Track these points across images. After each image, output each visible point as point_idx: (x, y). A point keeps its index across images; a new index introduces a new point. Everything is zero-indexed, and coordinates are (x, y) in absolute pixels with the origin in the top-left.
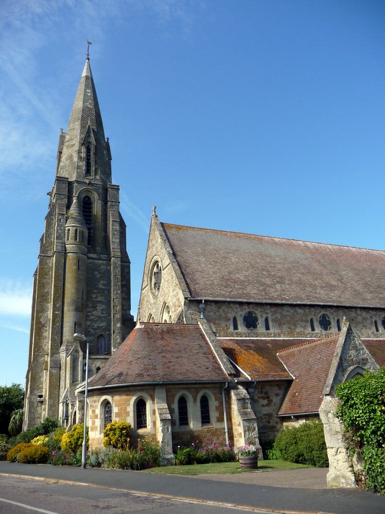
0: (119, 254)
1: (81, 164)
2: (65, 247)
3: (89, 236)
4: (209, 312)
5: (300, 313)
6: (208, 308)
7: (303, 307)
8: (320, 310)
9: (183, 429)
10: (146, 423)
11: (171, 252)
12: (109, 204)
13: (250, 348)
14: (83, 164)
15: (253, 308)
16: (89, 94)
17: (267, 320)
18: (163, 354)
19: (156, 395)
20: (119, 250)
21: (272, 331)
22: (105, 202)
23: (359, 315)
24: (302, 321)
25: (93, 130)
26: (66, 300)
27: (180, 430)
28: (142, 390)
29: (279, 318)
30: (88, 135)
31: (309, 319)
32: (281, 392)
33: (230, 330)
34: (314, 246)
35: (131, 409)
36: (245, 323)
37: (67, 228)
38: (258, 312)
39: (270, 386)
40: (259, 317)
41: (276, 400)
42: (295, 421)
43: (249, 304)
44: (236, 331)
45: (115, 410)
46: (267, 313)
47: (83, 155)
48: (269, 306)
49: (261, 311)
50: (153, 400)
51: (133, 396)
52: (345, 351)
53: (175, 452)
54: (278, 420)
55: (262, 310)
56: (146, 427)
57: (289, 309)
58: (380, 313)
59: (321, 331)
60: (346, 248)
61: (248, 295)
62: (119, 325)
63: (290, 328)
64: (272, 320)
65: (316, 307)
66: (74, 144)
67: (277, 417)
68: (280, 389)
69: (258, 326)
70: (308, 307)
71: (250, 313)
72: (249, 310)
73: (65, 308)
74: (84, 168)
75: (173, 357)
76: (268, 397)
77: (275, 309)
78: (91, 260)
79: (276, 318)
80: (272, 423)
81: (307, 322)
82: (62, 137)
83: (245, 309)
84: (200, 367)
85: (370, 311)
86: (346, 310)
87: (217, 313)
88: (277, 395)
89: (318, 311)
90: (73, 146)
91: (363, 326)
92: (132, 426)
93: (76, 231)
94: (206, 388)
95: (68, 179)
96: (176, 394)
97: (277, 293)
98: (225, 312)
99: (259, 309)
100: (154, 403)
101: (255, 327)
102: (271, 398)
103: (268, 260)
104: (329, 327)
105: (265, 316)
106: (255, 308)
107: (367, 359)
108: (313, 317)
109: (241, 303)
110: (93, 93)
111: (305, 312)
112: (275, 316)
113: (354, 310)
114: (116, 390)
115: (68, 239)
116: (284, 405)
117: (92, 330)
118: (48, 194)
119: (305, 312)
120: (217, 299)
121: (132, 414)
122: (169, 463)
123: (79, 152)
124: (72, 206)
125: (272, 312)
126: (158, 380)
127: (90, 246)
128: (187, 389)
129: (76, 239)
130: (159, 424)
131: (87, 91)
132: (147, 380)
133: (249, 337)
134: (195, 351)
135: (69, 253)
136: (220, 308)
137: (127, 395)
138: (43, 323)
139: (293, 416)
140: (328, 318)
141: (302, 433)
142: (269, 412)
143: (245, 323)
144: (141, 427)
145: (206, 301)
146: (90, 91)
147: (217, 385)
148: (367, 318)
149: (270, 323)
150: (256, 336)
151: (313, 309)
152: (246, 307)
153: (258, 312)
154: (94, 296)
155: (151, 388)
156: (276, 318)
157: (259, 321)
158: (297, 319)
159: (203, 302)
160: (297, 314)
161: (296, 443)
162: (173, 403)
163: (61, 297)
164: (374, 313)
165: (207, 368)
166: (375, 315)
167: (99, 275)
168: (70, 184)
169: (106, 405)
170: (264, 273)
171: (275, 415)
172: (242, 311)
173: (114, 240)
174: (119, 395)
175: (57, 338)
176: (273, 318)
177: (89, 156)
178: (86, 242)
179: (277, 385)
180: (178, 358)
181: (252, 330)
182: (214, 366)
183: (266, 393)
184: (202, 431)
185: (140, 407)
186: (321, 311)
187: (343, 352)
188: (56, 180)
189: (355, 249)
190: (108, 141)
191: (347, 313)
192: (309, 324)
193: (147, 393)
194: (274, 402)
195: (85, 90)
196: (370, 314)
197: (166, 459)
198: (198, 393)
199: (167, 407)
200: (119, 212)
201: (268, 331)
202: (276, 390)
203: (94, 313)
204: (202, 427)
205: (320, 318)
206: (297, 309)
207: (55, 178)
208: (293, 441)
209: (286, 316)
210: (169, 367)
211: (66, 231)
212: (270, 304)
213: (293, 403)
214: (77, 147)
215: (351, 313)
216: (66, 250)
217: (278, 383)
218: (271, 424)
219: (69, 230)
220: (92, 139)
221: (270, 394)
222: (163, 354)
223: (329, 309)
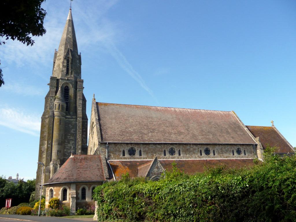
0: (81, 116)
1: (64, 69)
2: (54, 114)
3: (67, 107)
6: (110, 146)
7: (161, 145)
8: (170, 145)
9: (83, 201)
10: (66, 199)
11: (98, 118)
12: (78, 89)
14: (65, 69)
15: (133, 146)
16: (70, 30)
17: (140, 152)
18: (79, 170)
19: (71, 187)
20: (81, 114)
21: (142, 156)
22: (76, 88)
23: (191, 147)
24: (159, 151)
25: (71, 50)
27: (81, 202)
28: (66, 185)
30: (68, 53)
31: (163, 150)
33: (120, 156)
34: (180, 111)
35: (60, 193)
37: (55, 104)
38: (136, 148)
40: (136, 150)
43: (131, 144)
44: (124, 157)
45: (54, 193)
46: (141, 148)
47: (65, 64)
48: (142, 145)
49: (138, 147)
50: (70, 189)
51: (61, 187)
52: (152, 169)
53: (76, 210)
56: (66, 200)
57: (153, 145)
58: (204, 146)
60: (199, 110)
61: (132, 140)
63: (152, 155)
64: (143, 151)
65: (168, 144)
66: (61, 58)
69: (136, 154)
72: (131, 147)
74: (65, 71)
75: (83, 170)
77: (145, 146)
78: (67, 119)
79: (145, 150)
81: (162, 151)
82: (56, 54)
83: (129, 146)
84: (94, 175)
85: (198, 145)
86: (184, 145)
87: (115, 149)
89: (169, 146)
90: (60, 59)
91: (193, 153)
92: (60, 200)
93: (59, 105)
94: (95, 184)
95: (56, 78)
96: (80, 187)
97: (148, 138)
98: (119, 148)
99: (137, 146)
100: (70, 190)
101: (134, 154)
103: (150, 119)
104: (174, 154)
105: (139, 149)
106: (134, 145)
108: (166, 149)
109: (127, 144)
110: (72, 29)
111: (161, 147)
112: (145, 149)
113: (189, 145)
114: (56, 185)
115: (55, 109)
117: (67, 154)
118: (48, 85)
119: (161, 147)
120: (114, 142)
121: (60, 195)
122: (74, 214)
123: (63, 63)
125: (143, 147)
126: (72, 181)
127: (67, 112)
128: (86, 185)
129: (59, 109)
130: (71, 199)
131: (69, 28)
132: (68, 181)
133: (130, 159)
134: (94, 168)
136: (116, 146)
137: (59, 187)
138: (43, 150)
140: (174, 149)
144: (65, 200)
145: (108, 143)
146: (70, 28)
147: (100, 183)
148: (196, 149)
152: (130, 145)
153: (136, 148)
157: (136, 152)
158: (157, 150)
159: (107, 143)
160: (157, 148)
164: (201, 146)
165: (97, 175)
166: (200, 147)
168: (58, 80)
169: (51, 191)
170: (145, 127)
172: (127, 147)
173: (79, 109)
174: (56, 187)
176: (144, 150)
178: (65, 110)
180: (85, 171)
181: (132, 156)
182: (101, 174)
184: (91, 202)
185: (65, 192)
186: (170, 146)
189: (204, 111)
191: (185, 147)
192: (163, 153)
193: (67, 186)
196: (198, 147)
197: (72, 213)
199: (75, 192)
200: (83, 94)
201: (140, 157)
204: (92, 200)
205: (170, 149)
207: (50, 78)
209: (151, 149)
210: (79, 175)
211: (55, 105)
212: (143, 144)
214: (62, 60)
216: (54, 115)
219: (56, 105)
222: (79, 170)
223: (175, 145)
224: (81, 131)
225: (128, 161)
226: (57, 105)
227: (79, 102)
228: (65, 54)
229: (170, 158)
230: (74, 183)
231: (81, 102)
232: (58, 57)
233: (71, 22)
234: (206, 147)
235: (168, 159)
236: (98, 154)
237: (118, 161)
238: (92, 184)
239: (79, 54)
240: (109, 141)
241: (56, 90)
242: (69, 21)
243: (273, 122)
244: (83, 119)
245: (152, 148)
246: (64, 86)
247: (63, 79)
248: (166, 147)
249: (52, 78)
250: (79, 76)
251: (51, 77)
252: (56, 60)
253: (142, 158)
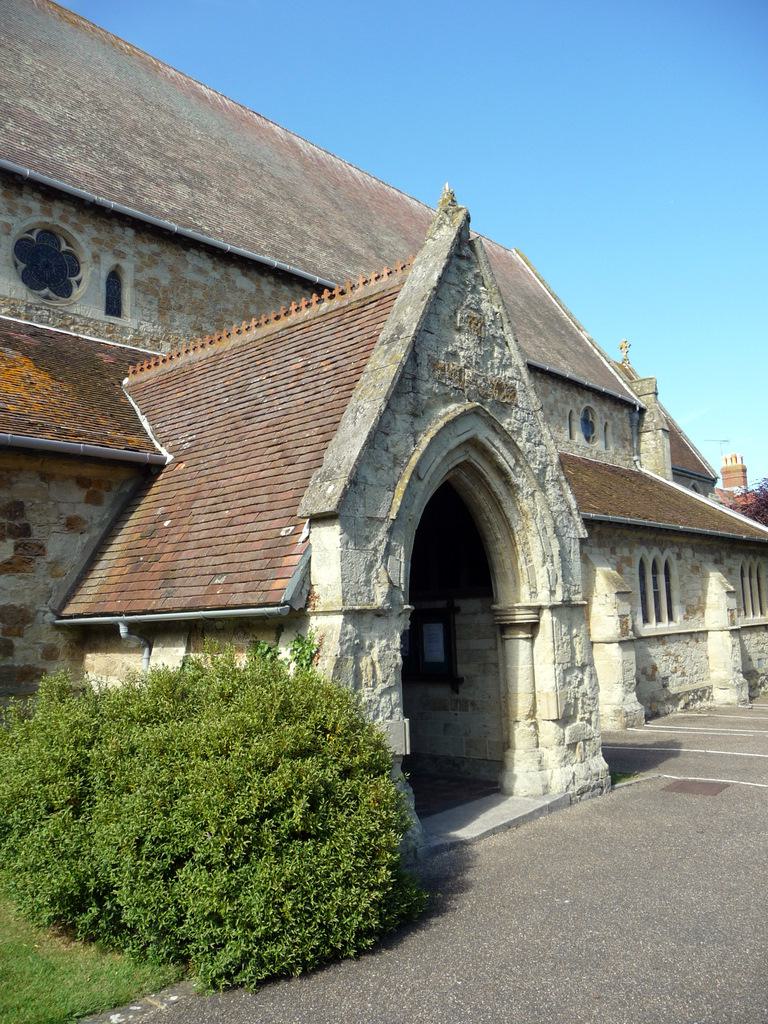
5: (243, 291)
13: (11, 343)
15: (63, 218)
17: (114, 280)
21: (129, 321)
29: (165, 282)
32: (97, 515)
34: (315, 154)
36: (23, 266)
38: (84, 240)
39: (45, 477)
40: (85, 254)
41: (63, 547)
42: (138, 649)
43: (50, 194)
46: (120, 254)
48: (130, 232)
49: (96, 240)
52: (434, 326)
54: (61, 641)
55: (104, 236)
57: (207, 264)
60: (396, 192)
61: (58, 169)
63: (200, 329)
67: (58, 627)
68: (93, 499)
69: (77, 292)
70: (272, 279)
71: (49, 234)
76: (26, 531)
77: (155, 247)
79: (154, 280)
80: (25, 653)
83: (29, 210)
88: (73, 524)
97: (173, 205)
101: (65, 291)
102: (37, 534)
103: (165, 119)
105: (108, 262)
106: (73, 219)
107: (513, 392)
111: (259, 290)
112: (149, 273)
116: (101, 571)
125: (140, 254)
139: (131, 626)
141: (137, 735)
142: (17, 603)
143: (23, 266)
149: (128, 295)
150: (58, 321)
152: (35, 205)
153: (84, 240)
156: (154, 280)
157: (85, 273)
158: (230, 307)
160: (234, 289)
161: (79, 803)
170: (142, 141)
171: (50, 617)
176: (143, 277)
179: (82, 482)
181: (47, 297)
183: (17, 509)
187: (424, 329)
189: (416, 203)
194: (51, 556)
201: (113, 319)
202: (72, 501)
206: (235, 273)
208: (61, 792)
209: (194, 285)
213: (137, 561)
217: (90, 471)
218: (18, 660)
221: (32, 517)
243: (626, 347)
245: (199, 279)
253: (124, 329)
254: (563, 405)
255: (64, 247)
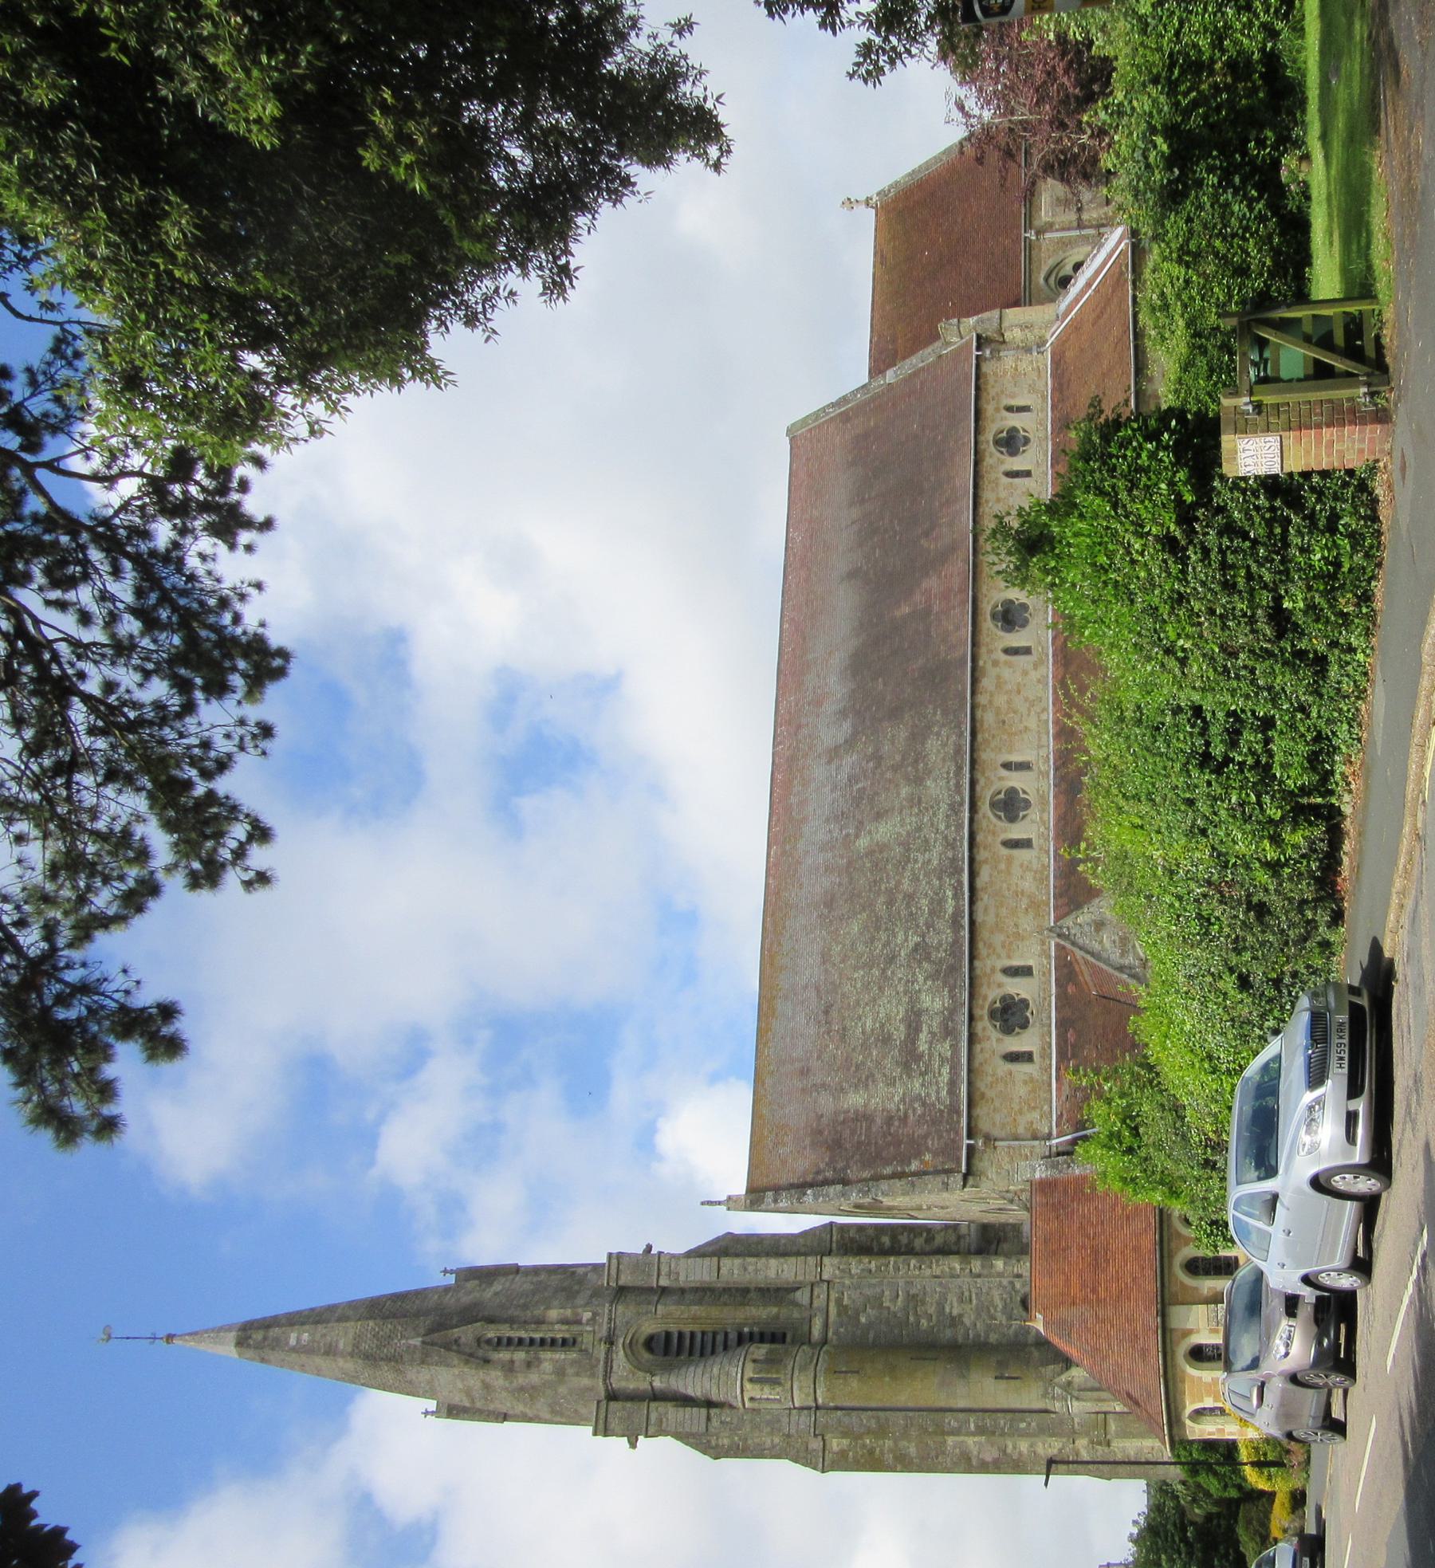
1: (547, 1366)
2: (802, 1408)
3: (762, 1338)
4: (994, 1124)
6: (984, 1125)
7: (976, 865)
11: (839, 1187)
12: (664, 1282)
14: (550, 1359)
15: (982, 1008)
23: (990, 702)
25: (430, 1331)
26: (942, 1404)
28: (1173, 1352)
29: (1002, 938)
31: (1005, 851)
33: (1036, 1075)
38: (992, 993)
43: (971, 1018)
44: (1036, 1057)
45: (1209, 1403)
46: (993, 970)
47: (520, 1356)
51: (1184, 1372)
55: (984, 981)
57: (980, 906)
59: (1033, 821)
62: (999, 1264)
64: (1009, 957)
65: (975, 826)
66: (483, 1381)
69: (1024, 995)
73: (962, 1404)
74: (560, 1356)
77: (980, 945)
78: (830, 1334)
83: (984, 1029)
85: (981, 663)
86: (980, 737)
87: (997, 1104)
89: (984, 824)
90: (487, 1386)
91: (1019, 692)
93: (751, 1380)
96: (1182, 1283)
100: (1198, 1331)
105: (1001, 978)
106: (981, 1002)
112: (999, 949)
113: (979, 713)
115: (779, 1401)
123: (509, 1368)
124: (682, 1390)
127: (789, 1339)
128: (1171, 1257)
129: (775, 1382)
131: (293, 1341)
132: (1154, 1344)
135: (816, 1399)
136: (983, 1095)
137: (1183, 1382)
145: (969, 1137)
148: (998, 677)
149: (1016, 962)
151: (979, 838)
153: (992, 993)
154: (924, 1322)
155: (1167, 1335)
162: (1196, 1289)
163: (933, 1415)
164: (983, 650)
166: (990, 652)
167: (869, 1310)
172: (989, 1038)
175: (1034, 1421)
176: (1003, 954)
177: (521, 1341)
188: (605, 1435)
190: (451, 1272)
192: (1016, 852)
195: (294, 1350)
196: (989, 666)
198: (1179, 1235)
199: (1202, 1308)
200: (690, 1254)
203: (967, 1321)
205: (999, 818)
207: (600, 1438)
209: (997, 916)
211: (756, 1405)
214: (495, 1377)
215: (986, 726)
216: (809, 1408)
219: (752, 1399)
220: (466, 1334)
224: (892, 1259)
225: (1058, 1036)
226: (753, 1394)
227: (733, 1270)
228: (455, 1359)
229: (1045, 817)
230: (1163, 1314)
231: (726, 1262)
232: (473, 1401)
233: (258, 1336)
234: (988, 625)
235: (1048, 829)
236: (1022, 1191)
237: (1058, 1089)
238: (1169, 1226)
239: (451, 1279)
240: (957, 1133)
241: (669, 1404)
242: (249, 1346)
244: (830, 1253)
245: (992, 911)
246: (646, 1356)
247: (606, 1363)
248: (990, 839)
249: (601, 1426)
250: (586, 1274)
251: (595, 1434)
252: (491, 1407)
254: (1001, 488)
255: (998, 1005)
